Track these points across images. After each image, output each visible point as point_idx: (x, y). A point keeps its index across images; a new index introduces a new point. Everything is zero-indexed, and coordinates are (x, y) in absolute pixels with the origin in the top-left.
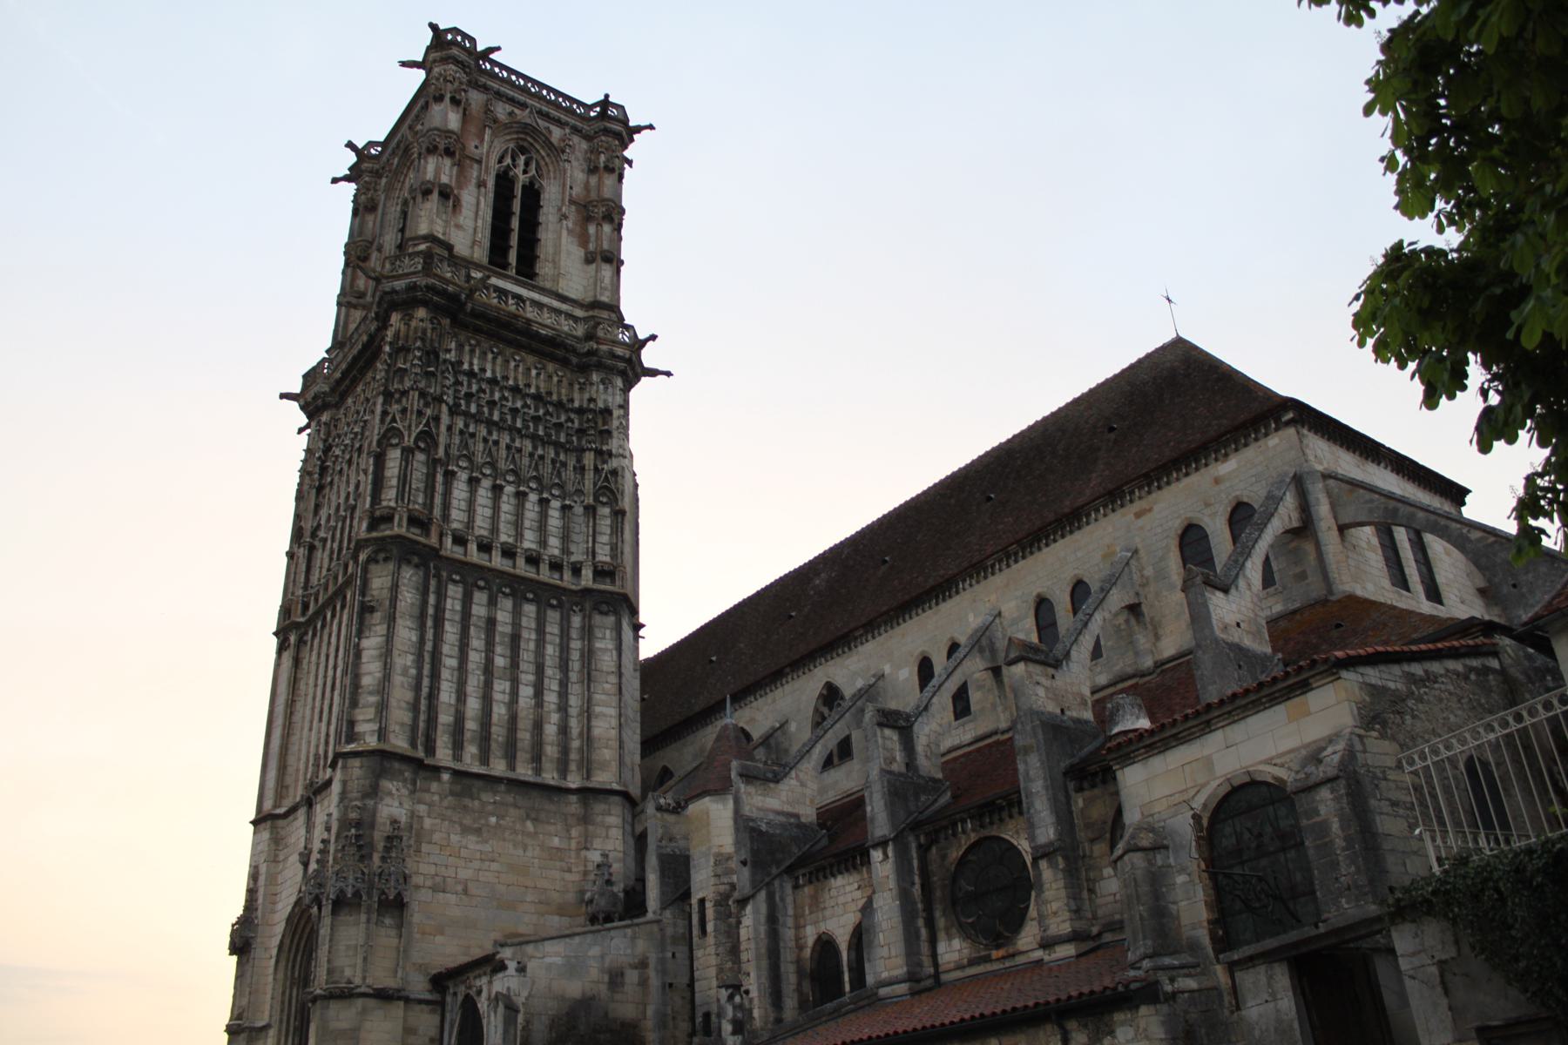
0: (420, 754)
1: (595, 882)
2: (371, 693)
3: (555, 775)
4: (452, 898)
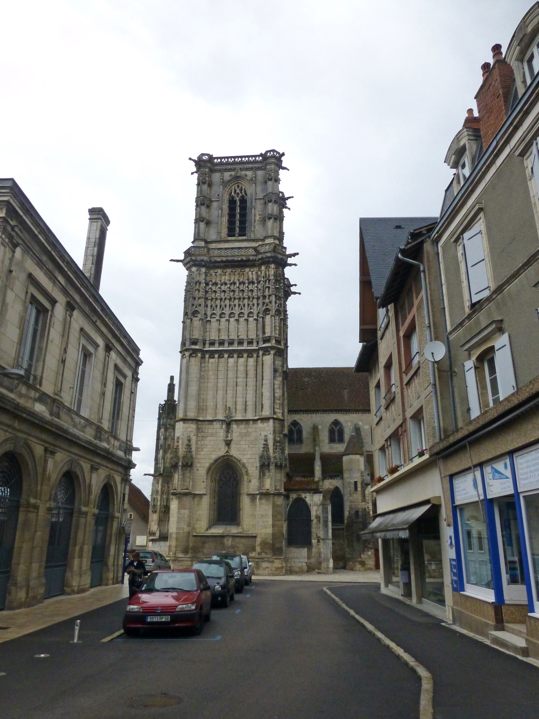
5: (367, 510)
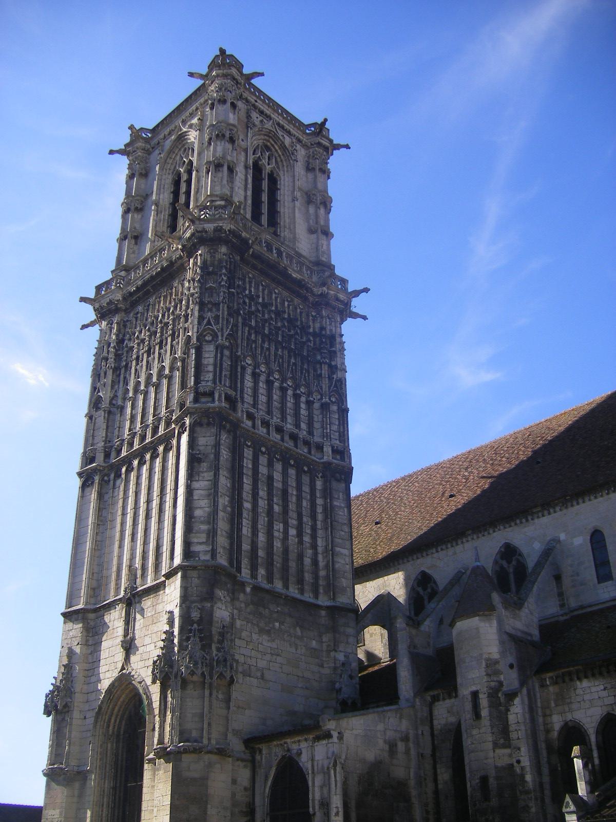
0: (234, 571)
1: (341, 676)
2: (202, 523)
3: (311, 595)
4: (255, 682)
5: (518, 771)
